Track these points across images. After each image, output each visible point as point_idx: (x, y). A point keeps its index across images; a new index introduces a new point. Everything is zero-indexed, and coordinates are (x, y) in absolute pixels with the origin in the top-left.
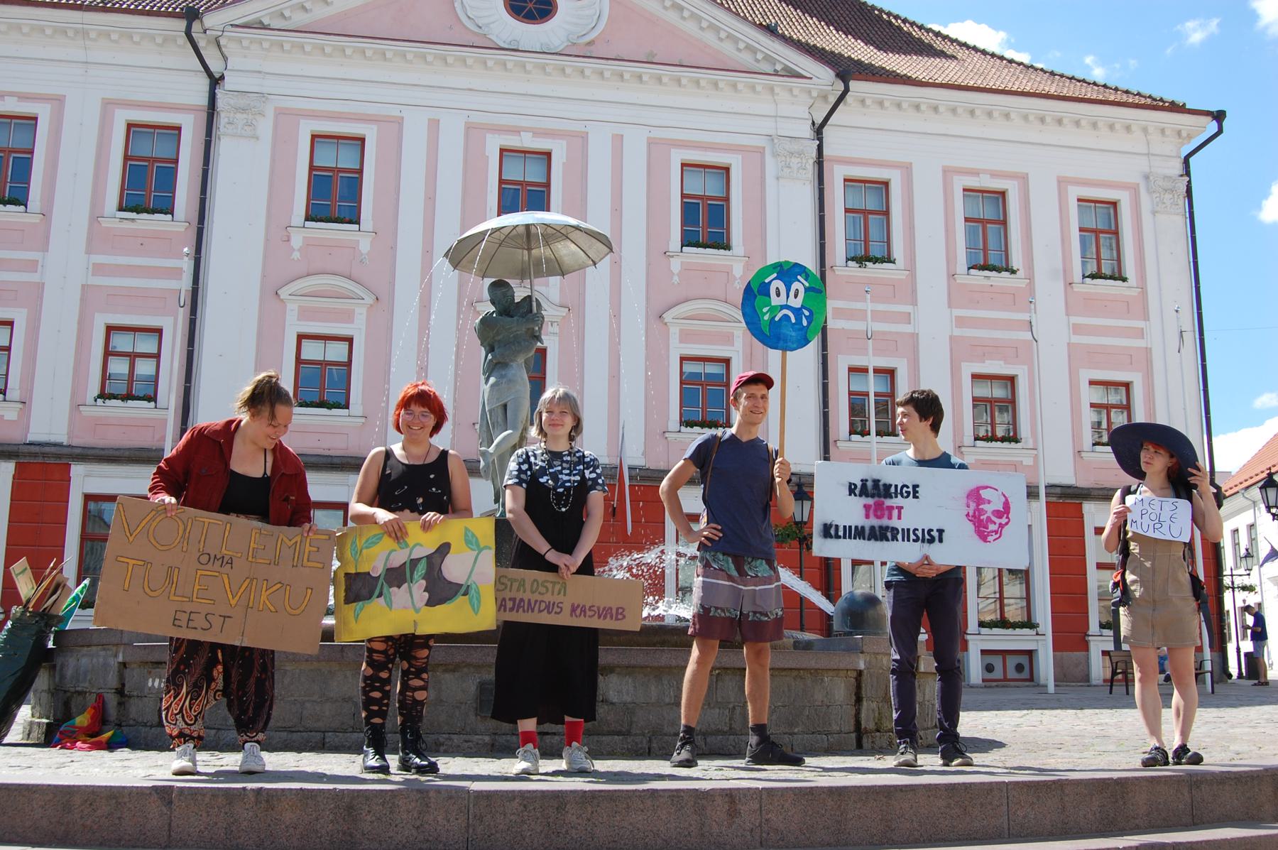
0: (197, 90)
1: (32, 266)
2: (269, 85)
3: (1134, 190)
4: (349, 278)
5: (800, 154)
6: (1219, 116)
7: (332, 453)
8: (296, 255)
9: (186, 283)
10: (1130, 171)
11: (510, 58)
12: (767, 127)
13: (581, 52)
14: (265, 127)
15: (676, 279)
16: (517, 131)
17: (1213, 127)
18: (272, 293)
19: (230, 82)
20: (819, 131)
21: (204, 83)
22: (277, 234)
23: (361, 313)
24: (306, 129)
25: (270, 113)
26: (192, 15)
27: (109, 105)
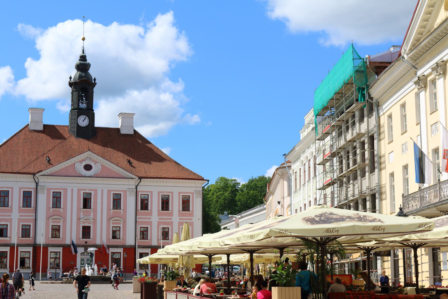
0: (34, 185)
1: (10, 216)
2: (46, 184)
3: (192, 193)
4: (59, 216)
5: (133, 191)
6: (208, 181)
7: (58, 244)
8: (51, 213)
9: (34, 218)
10: (192, 190)
11: (85, 178)
12: (127, 187)
14: (45, 191)
15: (112, 214)
16: (86, 190)
17: (207, 182)
18: (48, 218)
19: (40, 184)
20: (136, 187)
21: (35, 184)
22: (48, 209)
23: (61, 221)
24: (52, 191)
25: (46, 189)
26: (34, 174)
27: (20, 189)
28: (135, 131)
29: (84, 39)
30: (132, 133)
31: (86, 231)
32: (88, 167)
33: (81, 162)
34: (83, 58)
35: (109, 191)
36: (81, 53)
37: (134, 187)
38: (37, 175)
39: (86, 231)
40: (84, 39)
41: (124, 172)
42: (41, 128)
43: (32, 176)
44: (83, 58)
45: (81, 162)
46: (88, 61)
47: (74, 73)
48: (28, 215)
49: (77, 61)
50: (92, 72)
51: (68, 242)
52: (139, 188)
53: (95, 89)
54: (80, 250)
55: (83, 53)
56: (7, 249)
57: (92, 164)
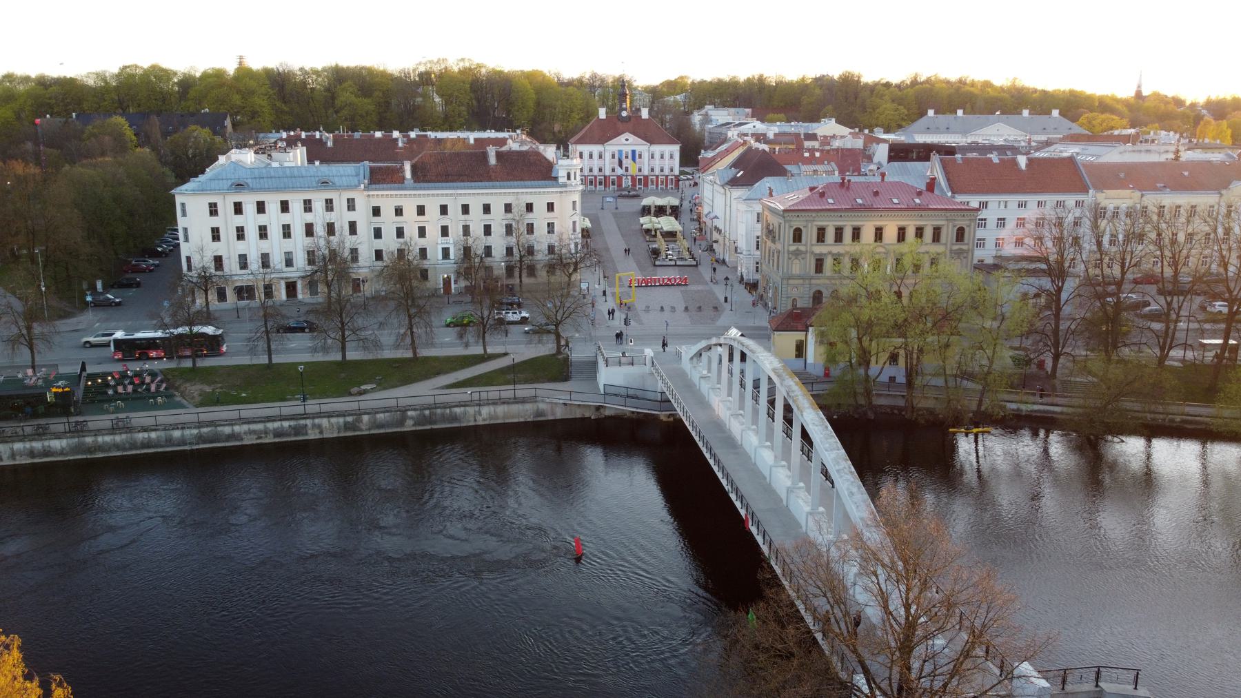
18: (610, 164)
32: (627, 140)
54: (624, 178)
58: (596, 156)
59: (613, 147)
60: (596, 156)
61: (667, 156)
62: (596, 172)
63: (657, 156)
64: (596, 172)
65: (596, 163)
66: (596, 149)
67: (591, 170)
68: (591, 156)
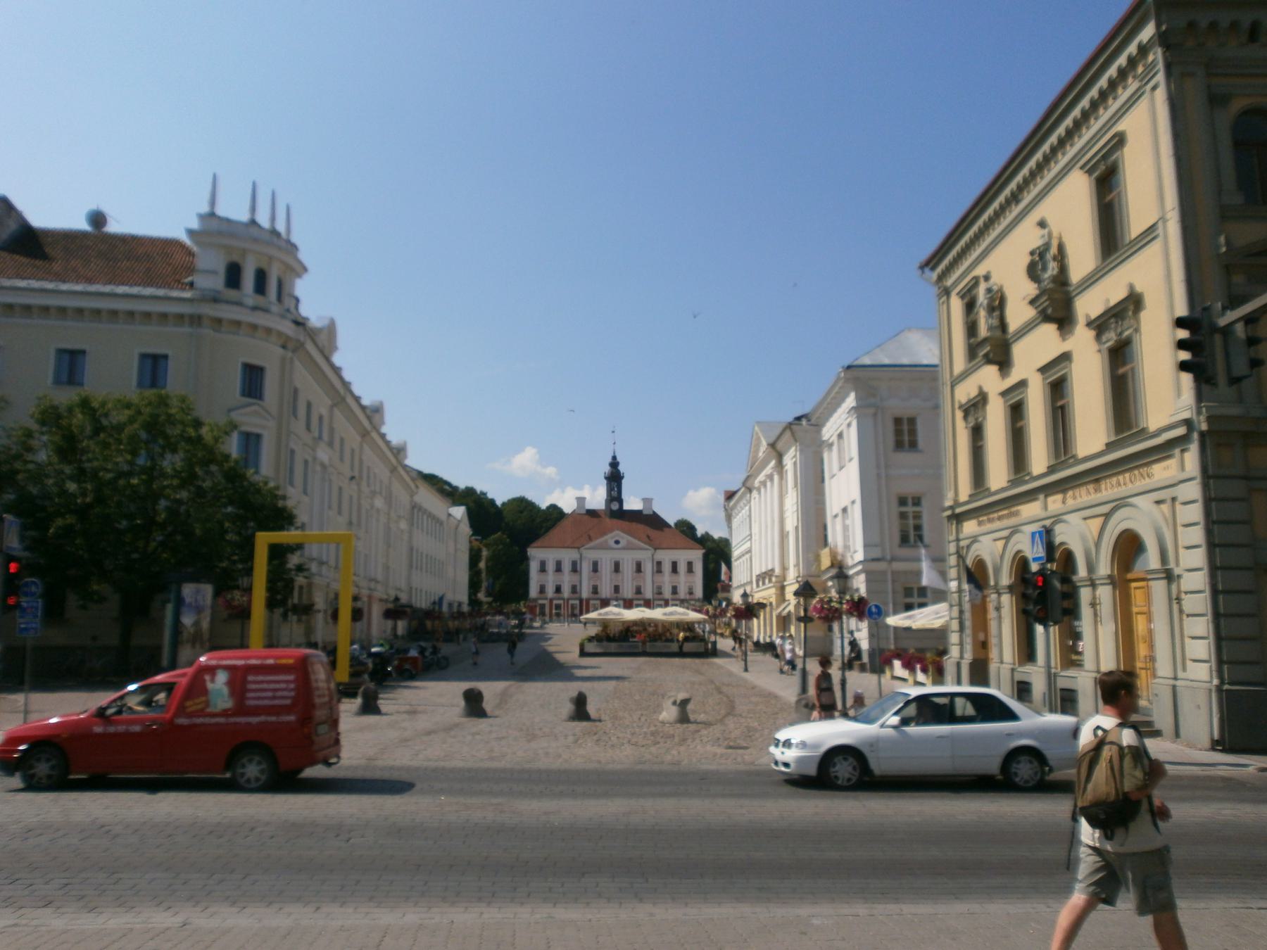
13: (624, 548)
18: (590, 579)
28: (654, 512)
29: (614, 443)
30: (651, 513)
31: (617, 589)
32: (617, 542)
33: (612, 538)
34: (614, 458)
35: (633, 559)
36: (612, 454)
37: (650, 556)
38: (582, 549)
39: (617, 589)
40: (614, 443)
41: (642, 544)
42: (584, 512)
43: (576, 550)
44: (614, 458)
45: (612, 538)
46: (619, 459)
47: (607, 469)
48: (575, 578)
49: (609, 460)
50: (621, 468)
51: (604, 596)
52: (655, 557)
53: (624, 482)
55: (614, 453)
56: (561, 602)
57: (620, 540)
58: (567, 567)
59: (590, 555)
60: (567, 567)
61: (682, 568)
62: (566, 592)
63: (667, 568)
64: (566, 592)
65: (567, 580)
66: (567, 556)
67: (558, 589)
68: (559, 568)
